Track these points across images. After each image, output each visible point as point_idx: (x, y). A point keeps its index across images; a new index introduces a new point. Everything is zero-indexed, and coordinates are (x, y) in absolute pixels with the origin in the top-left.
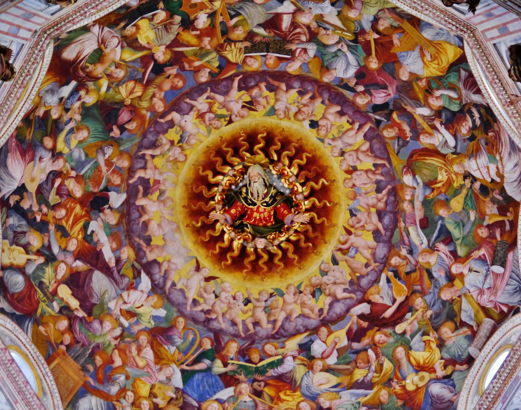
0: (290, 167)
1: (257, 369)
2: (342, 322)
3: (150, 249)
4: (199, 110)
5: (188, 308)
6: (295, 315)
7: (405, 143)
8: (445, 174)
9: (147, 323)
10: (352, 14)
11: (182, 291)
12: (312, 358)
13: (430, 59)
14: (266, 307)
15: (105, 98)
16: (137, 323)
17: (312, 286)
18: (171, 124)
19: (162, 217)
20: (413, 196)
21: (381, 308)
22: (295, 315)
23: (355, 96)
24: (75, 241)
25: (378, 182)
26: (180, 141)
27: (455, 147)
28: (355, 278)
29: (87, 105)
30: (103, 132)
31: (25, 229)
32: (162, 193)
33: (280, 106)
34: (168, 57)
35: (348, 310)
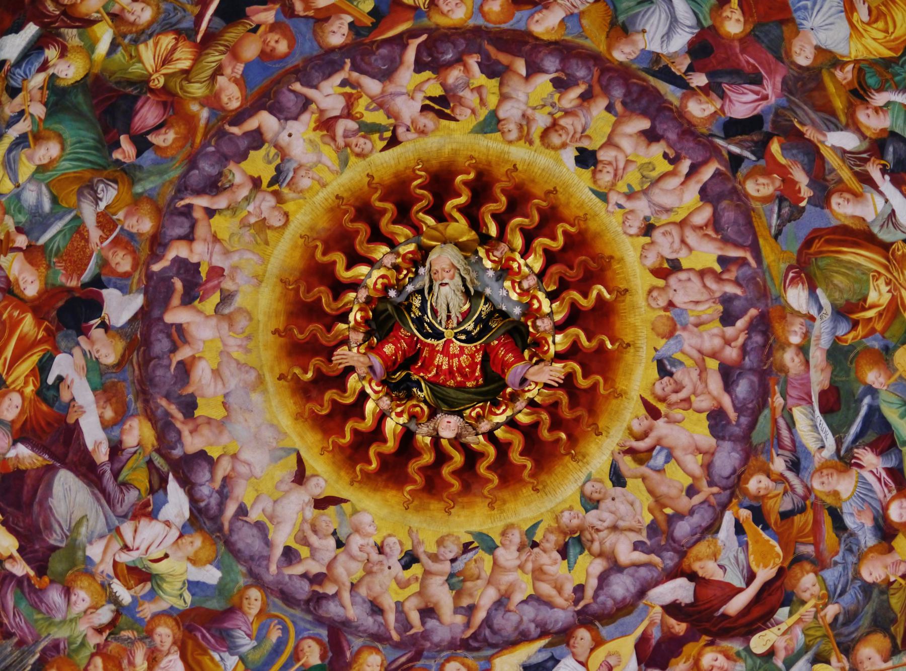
0: (525, 254)
2: (628, 619)
3: (191, 426)
4: (322, 111)
5: (273, 568)
6: (518, 597)
7: (797, 213)
8: (884, 289)
13: (866, 18)
14: (451, 575)
15: (104, 70)
16: (152, 596)
17: (561, 531)
18: (257, 139)
19: (224, 353)
20: (807, 336)
21: (718, 593)
22: (518, 597)
23: (684, 98)
24: (16, 399)
25: (726, 300)
26: (274, 181)
28: (661, 518)
29: (63, 84)
30: (96, 148)
32: (227, 298)
33: (510, 112)
35: (642, 593)
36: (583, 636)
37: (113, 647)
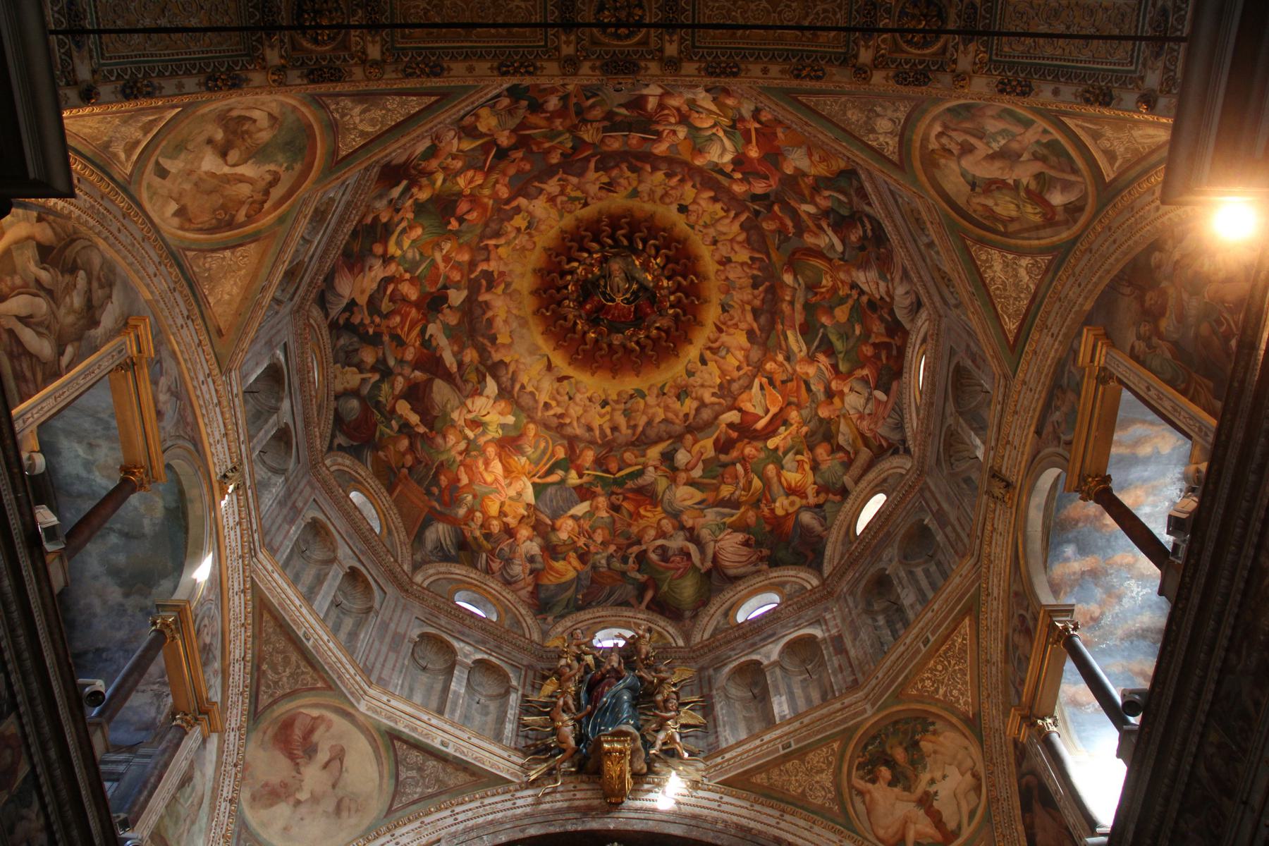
1: (615, 479)
4: (549, 194)
5: (539, 414)
6: (657, 420)
7: (787, 239)
9: (494, 433)
10: (730, 102)
11: (532, 394)
12: (675, 469)
16: (484, 433)
19: (509, 312)
20: (793, 296)
22: (657, 420)
24: (412, 349)
25: (754, 277)
26: (527, 228)
27: (843, 253)
31: (357, 346)
32: (508, 285)
33: (644, 188)
34: (513, 140)
35: (716, 417)
36: (689, 437)
37: (468, 460)
